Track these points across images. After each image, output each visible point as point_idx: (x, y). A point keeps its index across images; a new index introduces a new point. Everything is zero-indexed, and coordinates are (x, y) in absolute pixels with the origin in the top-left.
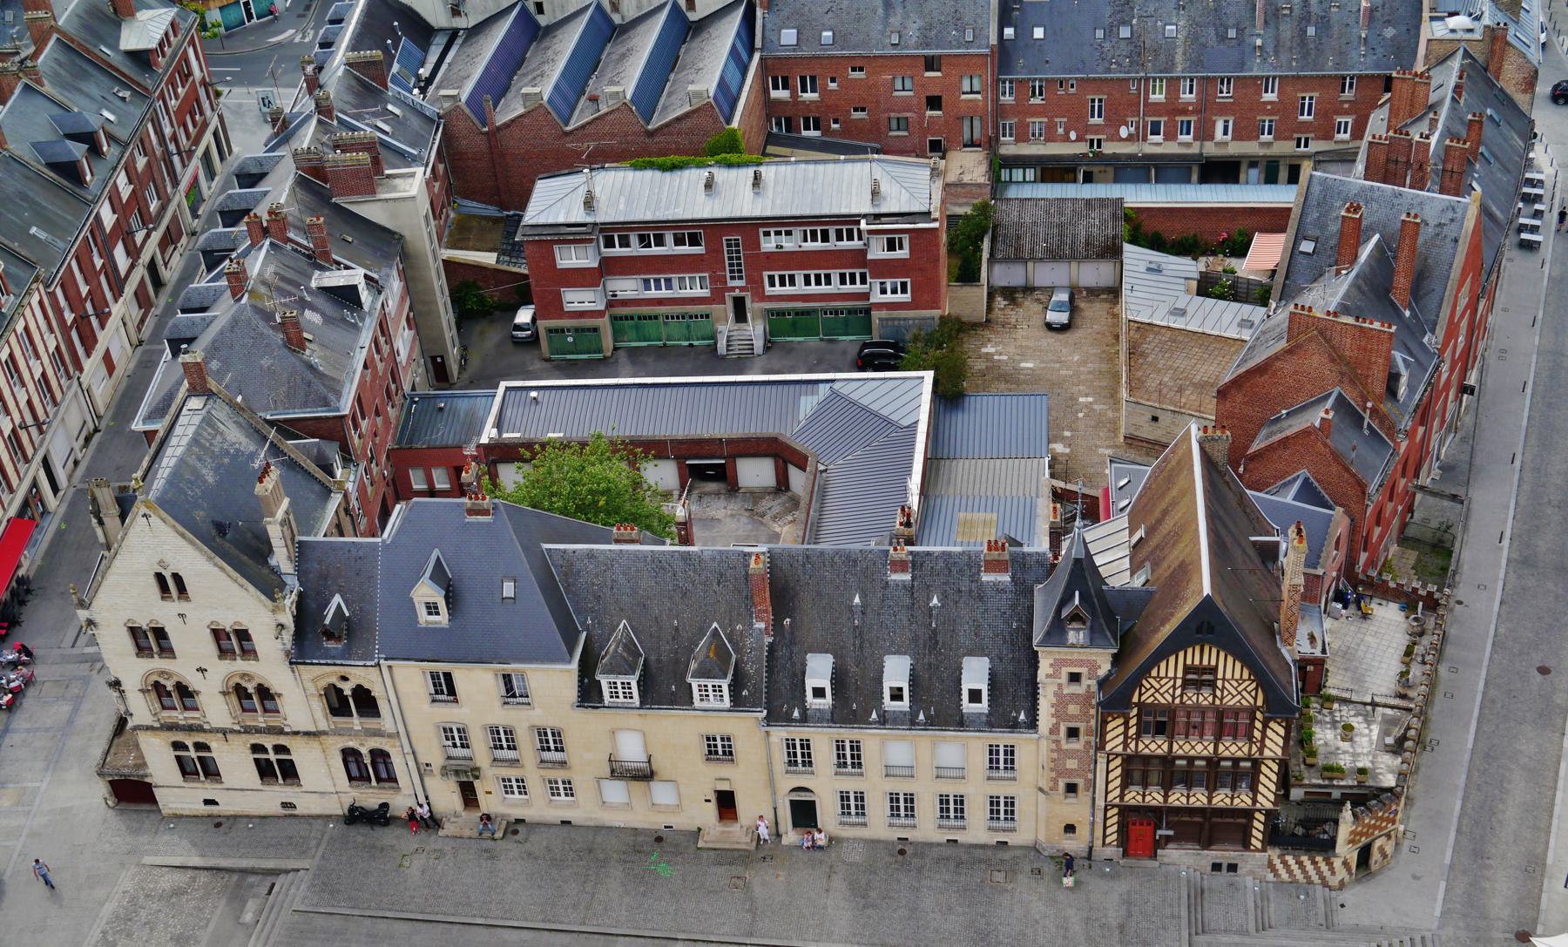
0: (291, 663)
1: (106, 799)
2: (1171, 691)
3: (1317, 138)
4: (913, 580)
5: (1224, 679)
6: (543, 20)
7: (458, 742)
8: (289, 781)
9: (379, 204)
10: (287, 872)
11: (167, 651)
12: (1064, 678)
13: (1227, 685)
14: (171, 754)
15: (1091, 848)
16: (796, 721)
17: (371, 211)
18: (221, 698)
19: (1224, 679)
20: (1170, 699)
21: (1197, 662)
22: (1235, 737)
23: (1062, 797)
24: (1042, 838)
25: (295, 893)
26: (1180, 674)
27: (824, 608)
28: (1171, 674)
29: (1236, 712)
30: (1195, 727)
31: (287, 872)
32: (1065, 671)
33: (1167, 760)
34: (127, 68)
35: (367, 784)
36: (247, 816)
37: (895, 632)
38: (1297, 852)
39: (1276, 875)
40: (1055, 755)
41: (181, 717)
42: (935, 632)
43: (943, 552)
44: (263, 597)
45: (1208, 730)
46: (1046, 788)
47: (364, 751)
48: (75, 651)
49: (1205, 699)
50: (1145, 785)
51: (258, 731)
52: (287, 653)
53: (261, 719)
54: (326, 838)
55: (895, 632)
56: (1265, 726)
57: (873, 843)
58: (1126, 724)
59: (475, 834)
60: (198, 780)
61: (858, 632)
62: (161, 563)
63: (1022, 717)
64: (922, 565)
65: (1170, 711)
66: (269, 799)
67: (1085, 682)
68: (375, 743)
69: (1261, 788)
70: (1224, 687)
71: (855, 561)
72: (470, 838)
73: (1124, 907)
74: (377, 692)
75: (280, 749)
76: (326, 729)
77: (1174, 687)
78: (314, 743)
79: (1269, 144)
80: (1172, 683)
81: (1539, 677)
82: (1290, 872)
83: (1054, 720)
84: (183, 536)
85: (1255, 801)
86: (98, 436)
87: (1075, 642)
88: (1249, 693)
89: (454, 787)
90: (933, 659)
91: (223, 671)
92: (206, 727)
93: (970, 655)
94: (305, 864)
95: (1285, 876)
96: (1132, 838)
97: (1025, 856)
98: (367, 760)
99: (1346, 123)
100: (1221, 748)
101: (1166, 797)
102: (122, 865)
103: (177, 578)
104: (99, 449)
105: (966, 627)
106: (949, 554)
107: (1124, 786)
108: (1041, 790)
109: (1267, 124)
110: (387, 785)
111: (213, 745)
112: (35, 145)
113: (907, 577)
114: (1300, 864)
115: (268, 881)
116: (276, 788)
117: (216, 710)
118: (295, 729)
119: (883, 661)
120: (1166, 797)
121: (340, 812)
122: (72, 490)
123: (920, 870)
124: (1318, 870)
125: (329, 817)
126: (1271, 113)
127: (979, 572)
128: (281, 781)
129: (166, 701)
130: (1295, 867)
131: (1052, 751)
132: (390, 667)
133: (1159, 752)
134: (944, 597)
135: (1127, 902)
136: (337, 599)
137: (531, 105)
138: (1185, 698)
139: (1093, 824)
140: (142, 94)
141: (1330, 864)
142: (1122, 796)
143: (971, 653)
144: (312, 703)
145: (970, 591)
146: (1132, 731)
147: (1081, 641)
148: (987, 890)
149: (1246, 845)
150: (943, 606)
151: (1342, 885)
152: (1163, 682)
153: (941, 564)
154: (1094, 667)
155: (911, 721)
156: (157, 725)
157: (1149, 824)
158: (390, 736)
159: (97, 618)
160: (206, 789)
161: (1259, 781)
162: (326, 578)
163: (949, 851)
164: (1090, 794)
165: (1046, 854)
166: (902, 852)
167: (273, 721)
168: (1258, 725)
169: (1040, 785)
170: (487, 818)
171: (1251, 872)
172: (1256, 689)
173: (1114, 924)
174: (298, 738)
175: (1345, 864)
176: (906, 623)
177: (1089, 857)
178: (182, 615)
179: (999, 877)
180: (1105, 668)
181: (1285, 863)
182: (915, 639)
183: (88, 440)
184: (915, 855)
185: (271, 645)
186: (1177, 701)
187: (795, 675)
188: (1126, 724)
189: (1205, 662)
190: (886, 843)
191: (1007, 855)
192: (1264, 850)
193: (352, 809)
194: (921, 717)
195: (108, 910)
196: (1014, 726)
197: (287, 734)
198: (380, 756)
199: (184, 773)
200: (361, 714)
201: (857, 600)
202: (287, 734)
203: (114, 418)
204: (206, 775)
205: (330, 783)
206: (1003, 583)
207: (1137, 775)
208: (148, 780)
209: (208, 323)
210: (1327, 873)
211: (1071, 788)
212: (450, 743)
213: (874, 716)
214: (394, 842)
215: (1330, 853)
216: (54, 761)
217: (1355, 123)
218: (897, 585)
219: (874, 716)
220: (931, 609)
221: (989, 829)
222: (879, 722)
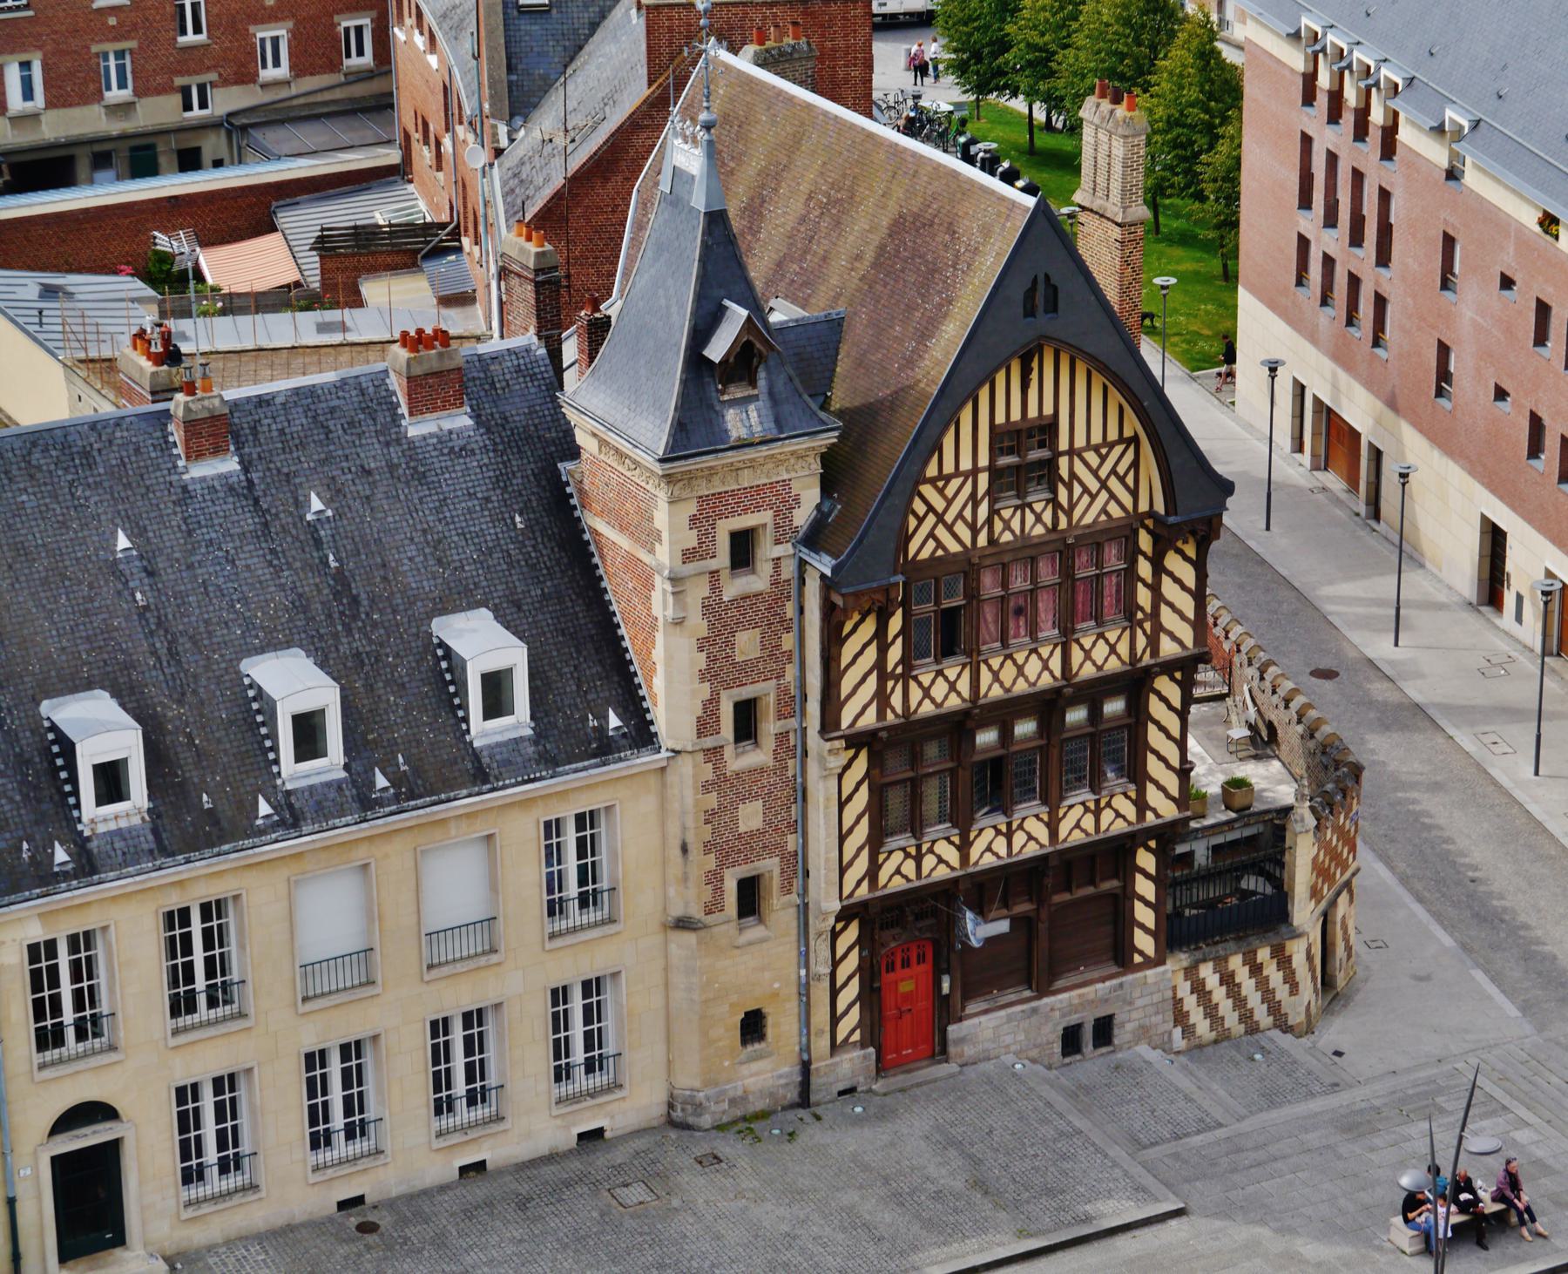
2: (968, 513)
3: (225, 82)
4: (246, 466)
5: (1072, 452)
12: (723, 559)
13: (1079, 468)
15: (806, 1067)
16: (65, 876)
19: (1072, 452)
20: (965, 534)
21: (1016, 415)
22: (1100, 622)
23: (732, 928)
24: (688, 1080)
26: (984, 461)
27: (45, 582)
28: (966, 464)
29: (1096, 539)
30: (1019, 611)
32: (725, 528)
33: (957, 726)
37: (244, 600)
38: (1220, 950)
39: (1188, 1031)
40: (712, 800)
42: (340, 576)
43: (296, 391)
45: (1046, 608)
46: (696, 912)
49: (1038, 519)
50: (916, 826)
55: (244, 600)
56: (1159, 568)
57: (281, 1236)
58: (880, 634)
61: (153, 620)
63: (614, 721)
64: (254, 431)
65: (967, 567)
67: (768, 550)
69: (1154, 766)
70: (1073, 475)
71: (86, 454)
73: (952, 1153)
77: (974, 500)
79: (125, 108)
80: (968, 488)
81: (1327, 685)
82: (1211, 1012)
83: (705, 690)
85: (1142, 805)
87: (743, 433)
88: (1122, 480)
90: (360, 643)
93: (444, 611)
95: (1203, 1027)
96: (891, 1012)
97: (660, 1145)
99: (275, 41)
100: (1077, 655)
101: (964, 847)
105: (412, 551)
106: (311, 392)
107: (875, 843)
108: (683, 924)
109: (112, 63)
113: (229, 465)
114: (1228, 980)
119: (240, 676)
120: (964, 847)
123: (440, 1242)
124: (1263, 985)
126: (117, 34)
127: (396, 419)
130: (1219, 994)
131: (706, 787)
133: (954, 702)
134: (334, 494)
135: (946, 1141)
138: (998, 525)
139: (805, 991)
141: (1284, 962)
142: (872, 873)
143: (446, 606)
145: (392, 467)
146: (895, 653)
147: (757, 429)
148: (629, 1223)
149: (1121, 955)
150: (339, 514)
151: (1309, 1029)
152: (950, 491)
153: (300, 421)
154: (785, 503)
155: (367, 803)
157: (921, 959)
161: (1147, 747)
163: (478, 1190)
164: (794, 898)
165: (706, 1121)
166: (366, 1228)
168: (1144, 569)
169: (677, 911)
171: (1144, 1033)
172: (1135, 464)
173: (958, 1184)
175: (1310, 958)
176: (265, 573)
177: (804, 1099)
179: (636, 1193)
180: (810, 497)
181: (1199, 989)
182: (301, 605)
184: (404, 1222)
186: (982, 540)
187: (22, 762)
188: (881, 633)
189: (1033, 413)
190: (316, 1226)
191: (602, 1159)
192: (1159, 961)
194: (381, 781)
196: (604, 748)
201: (123, 542)
206: (460, 432)
207: (896, 801)
210: (1282, 993)
211: (750, 898)
213: (264, 808)
215: (1283, 929)
217: (295, 36)
218: (212, 489)
219: (264, 808)
220: (312, 528)
221: (559, 1102)
222: (282, 824)
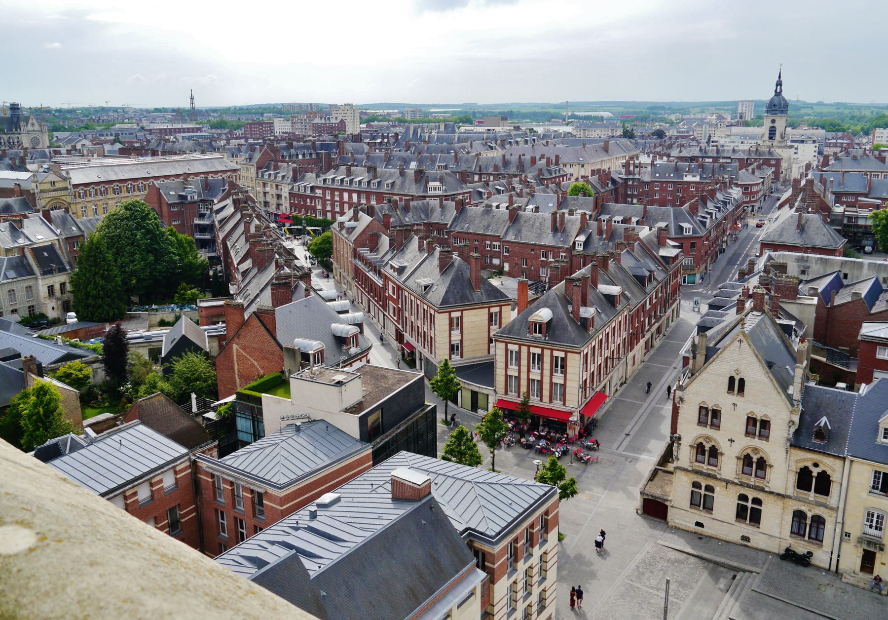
0: (791, 445)
1: (637, 510)
6: (845, 282)
7: (874, 524)
8: (753, 524)
9: (796, 305)
10: (744, 571)
11: (717, 427)
14: (690, 488)
17: (791, 308)
18: (735, 460)
25: (755, 582)
31: (744, 571)
34: (661, 260)
35: (802, 538)
36: (718, 539)
41: (705, 467)
44: (788, 403)
47: (809, 515)
48: (617, 452)
51: (749, 486)
52: (788, 440)
53: (753, 479)
54: (768, 562)
59: (868, 587)
60: (699, 510)
62: (737, 371)
66: (736, 531)
68: (819, 511)
72: (864, 589)
74: (835, 477)
75: (757, 501)
76: (791, 495)
78: (780, 503)
84: (757, 356)
86: (625, 385)
89: (861, 553)
91: (744, 443)
92: (718, 476)
94: (758, 570)
98: (809, 522)
102: (647, 540)
103: (742, 382)
104: (626, 388)
110: (814, 542)
111: (717, 489)
112: (629, 267)
115: (732, 573)
116: (743, 525)
117: (729, 467)
118: (772, 490)
121: (776, 551)
122: (614, 399)
125: (768, 552)
128: (748, 522)
129: (700, 457)
132: (852, 461)
136: (824, 419)
137: (855, 298)
140: (666, 271)
144: (790, 476)
156: (690, 469)
158: (831, 509)
159: (685, 398)
160: (700, 515)
162: (819, 407)
167: (759, 483)
170: (878, 579)
174: (771, 496)
178: (734, 405)
183: (621, 385)
185: (780, 432)
193: (788, 550)
195: (639, 557)
197: (766, 492)
198: (819, 521)
199: (691, 504)
200: (816, 491)
202: (766, 492)
203: (633, 380)
204: (704, 508)
205: (778, 530)
208: (667, 503)
209: (720, 322)
212: (868, 524)
214: (812, 576)
216: (609, 485)
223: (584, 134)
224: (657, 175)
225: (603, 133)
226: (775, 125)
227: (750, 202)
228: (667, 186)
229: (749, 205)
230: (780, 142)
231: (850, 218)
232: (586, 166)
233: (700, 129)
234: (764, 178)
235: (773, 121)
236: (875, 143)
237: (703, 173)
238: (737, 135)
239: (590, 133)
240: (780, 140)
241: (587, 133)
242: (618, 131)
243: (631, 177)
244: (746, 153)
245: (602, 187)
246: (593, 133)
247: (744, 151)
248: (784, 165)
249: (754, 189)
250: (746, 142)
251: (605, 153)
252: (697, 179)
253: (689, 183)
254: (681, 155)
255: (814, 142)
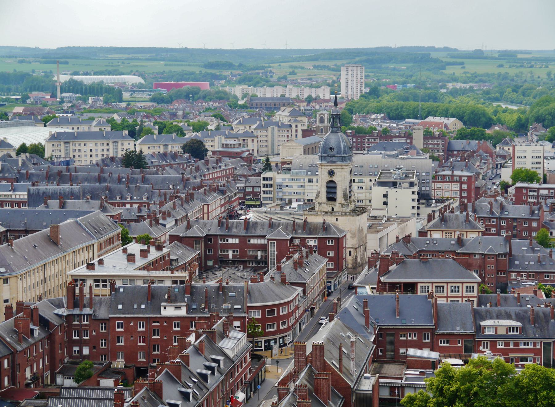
223: (67, 149)
224: (120, 307)
225: (99, 147)
226: (333, 179)
227: (279, 331)
228: (135, 325)
229: (277, 337)
230: (343, 205)
231: (392, 388)
232: (12, 281)
233: (264, 134)
234: (303, 285)
235: (331, 173)
236: (517, 166)
237: (193, 301)
238: (301, 168)
239: (77, 148)
240: (343, 202)
241: (71, 148)
242: (126, 143)
243: (77, 311)
244: (290, 228)
245: (20, 340)
246: (83, 147)
247: (286, 226)
248: (350, 242)
249: (284, 312)
250: (315, 180)
251: (52, 248)
252: (183, 312)
253: (170, 319)
254: (190, 233)
255: (412, 184)
